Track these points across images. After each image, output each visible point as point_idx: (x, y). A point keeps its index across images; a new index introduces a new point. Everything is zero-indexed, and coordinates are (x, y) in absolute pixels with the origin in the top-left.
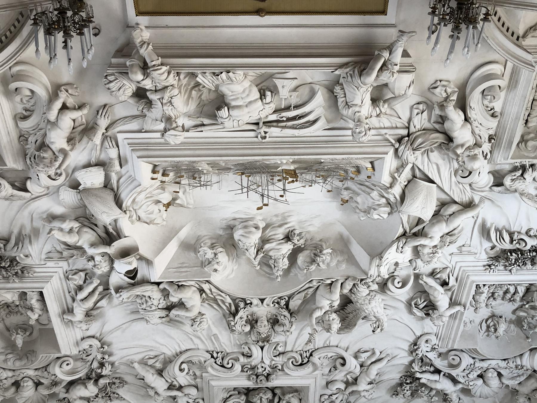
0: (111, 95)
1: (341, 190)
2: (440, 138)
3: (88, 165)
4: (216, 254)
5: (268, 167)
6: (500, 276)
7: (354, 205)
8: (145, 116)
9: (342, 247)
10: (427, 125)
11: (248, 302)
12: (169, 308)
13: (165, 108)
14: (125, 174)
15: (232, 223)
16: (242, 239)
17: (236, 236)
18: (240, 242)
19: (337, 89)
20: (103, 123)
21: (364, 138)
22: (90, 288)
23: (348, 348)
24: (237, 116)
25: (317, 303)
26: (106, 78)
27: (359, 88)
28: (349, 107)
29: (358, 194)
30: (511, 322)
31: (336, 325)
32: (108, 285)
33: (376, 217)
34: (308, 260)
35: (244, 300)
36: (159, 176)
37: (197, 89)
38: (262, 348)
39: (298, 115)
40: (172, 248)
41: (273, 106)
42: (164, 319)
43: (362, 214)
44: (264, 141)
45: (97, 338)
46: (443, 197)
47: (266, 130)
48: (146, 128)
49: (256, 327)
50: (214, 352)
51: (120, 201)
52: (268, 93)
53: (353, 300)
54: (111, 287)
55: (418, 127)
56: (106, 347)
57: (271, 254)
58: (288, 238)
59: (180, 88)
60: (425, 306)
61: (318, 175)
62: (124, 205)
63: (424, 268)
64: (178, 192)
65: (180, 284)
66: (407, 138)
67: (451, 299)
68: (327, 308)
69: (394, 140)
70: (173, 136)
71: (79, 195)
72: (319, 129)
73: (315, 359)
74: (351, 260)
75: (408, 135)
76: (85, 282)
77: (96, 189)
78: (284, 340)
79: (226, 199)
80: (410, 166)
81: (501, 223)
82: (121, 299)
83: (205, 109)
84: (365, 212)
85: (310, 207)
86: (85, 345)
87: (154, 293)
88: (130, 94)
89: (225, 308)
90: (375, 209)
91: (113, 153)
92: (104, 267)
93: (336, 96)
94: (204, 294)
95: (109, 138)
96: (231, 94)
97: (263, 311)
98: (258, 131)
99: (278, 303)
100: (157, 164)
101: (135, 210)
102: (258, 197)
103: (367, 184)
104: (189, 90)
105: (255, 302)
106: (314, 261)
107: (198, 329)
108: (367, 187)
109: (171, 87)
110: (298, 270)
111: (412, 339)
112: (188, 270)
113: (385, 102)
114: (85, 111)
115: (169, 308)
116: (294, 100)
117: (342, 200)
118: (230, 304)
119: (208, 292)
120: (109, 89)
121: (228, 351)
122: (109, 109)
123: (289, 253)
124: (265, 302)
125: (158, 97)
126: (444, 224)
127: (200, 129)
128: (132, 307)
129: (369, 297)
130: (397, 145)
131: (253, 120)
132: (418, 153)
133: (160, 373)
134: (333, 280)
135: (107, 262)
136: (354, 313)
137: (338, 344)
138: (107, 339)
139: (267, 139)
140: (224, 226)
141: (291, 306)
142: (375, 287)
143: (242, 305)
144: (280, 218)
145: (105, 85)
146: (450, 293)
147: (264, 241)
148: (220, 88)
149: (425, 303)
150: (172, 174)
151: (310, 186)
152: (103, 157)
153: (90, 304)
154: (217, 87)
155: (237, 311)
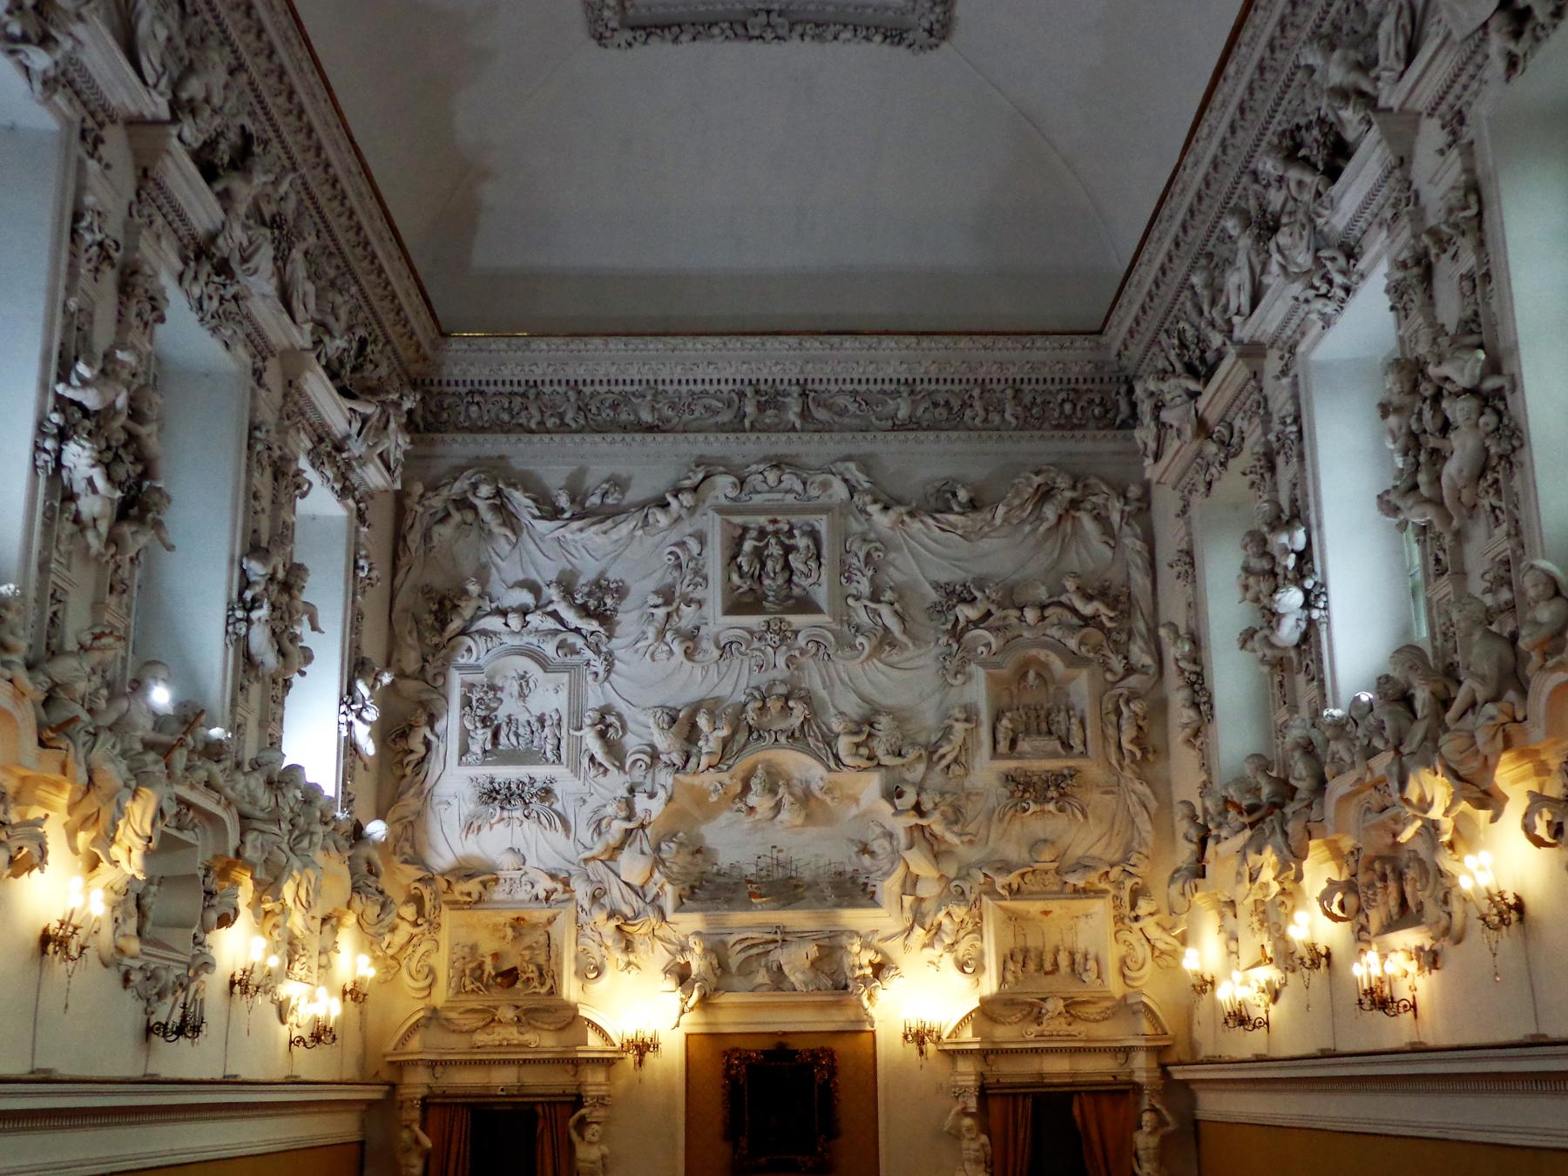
6: (540, 772)
19: (718, 972)
22: (944, 763)
30: (501, 689)
41: (772, 957)
46: (610, 863)
63: (616, 783)
81: (549, 834)
111: (613, 676)
115: (870, 735)
142: (664, 757)
143: (797, 734)
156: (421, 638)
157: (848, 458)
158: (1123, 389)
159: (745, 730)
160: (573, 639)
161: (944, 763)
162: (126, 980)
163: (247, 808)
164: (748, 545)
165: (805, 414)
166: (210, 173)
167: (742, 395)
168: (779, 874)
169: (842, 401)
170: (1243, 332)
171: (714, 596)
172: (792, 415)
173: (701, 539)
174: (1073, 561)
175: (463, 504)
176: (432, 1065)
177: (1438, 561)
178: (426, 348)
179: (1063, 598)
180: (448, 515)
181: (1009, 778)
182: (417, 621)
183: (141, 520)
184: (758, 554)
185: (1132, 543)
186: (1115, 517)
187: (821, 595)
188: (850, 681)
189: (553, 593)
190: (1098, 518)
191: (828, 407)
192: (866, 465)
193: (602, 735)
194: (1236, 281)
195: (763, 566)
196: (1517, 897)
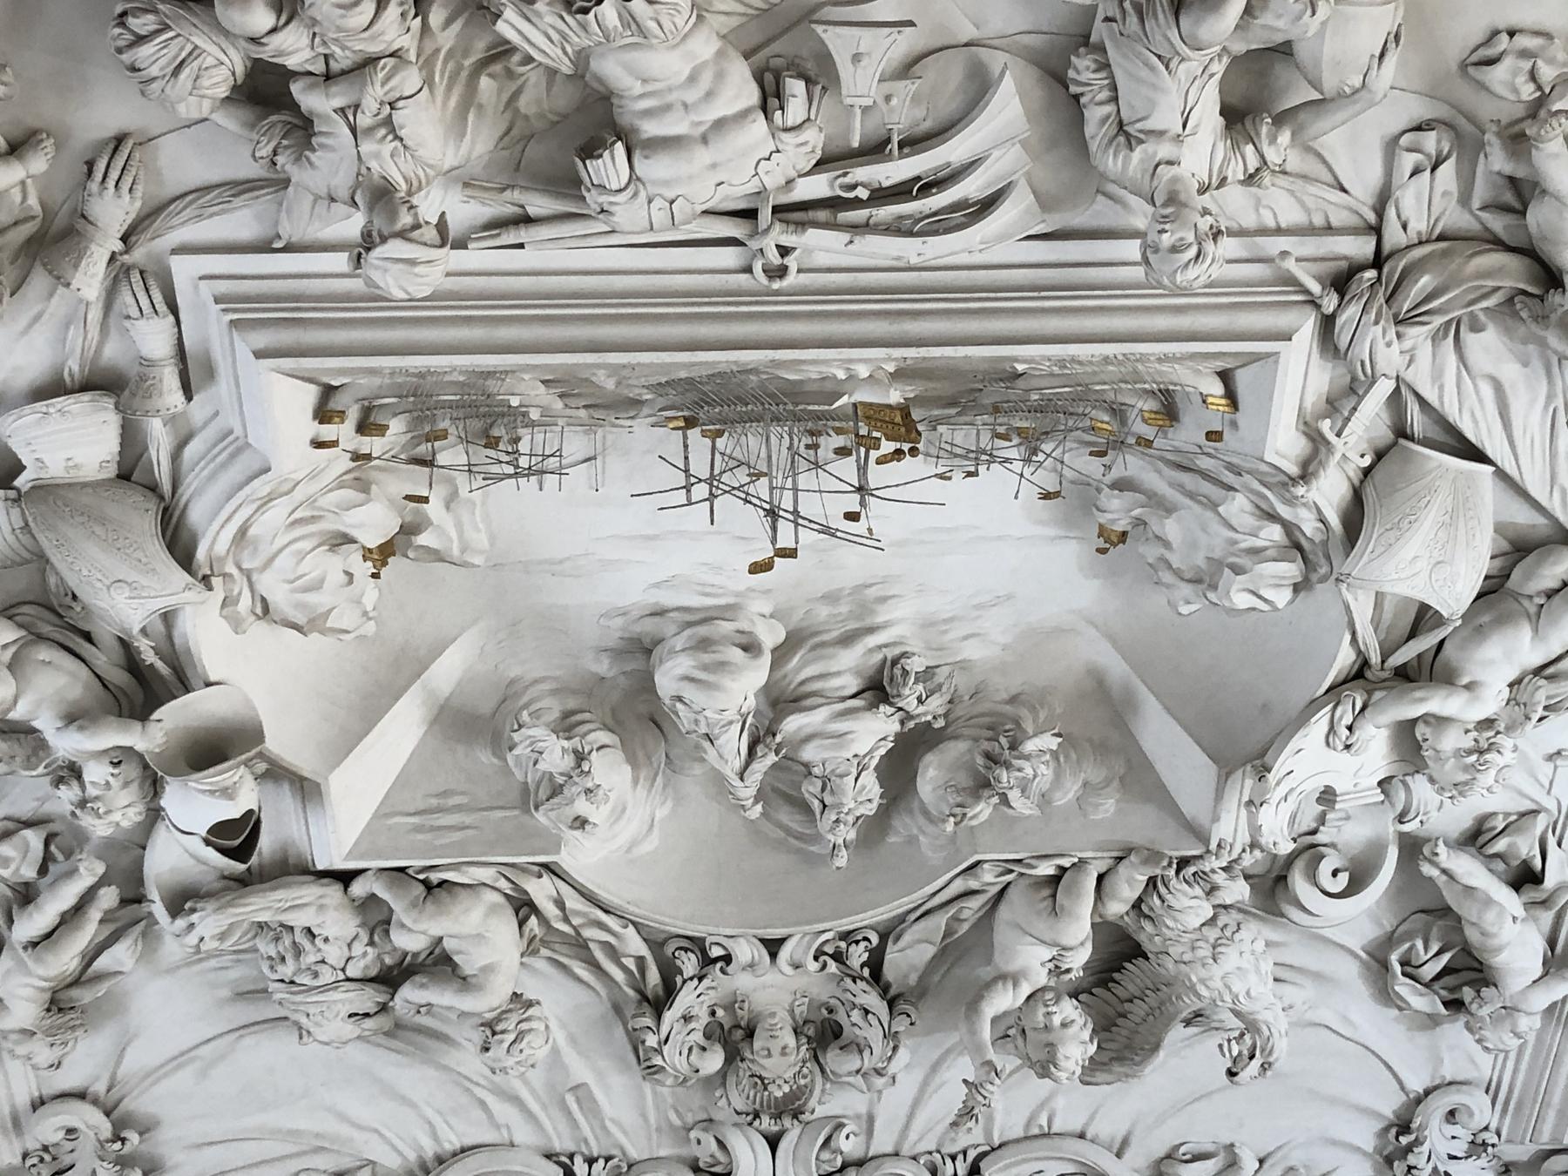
0: (143, 93)
1: (1099, 490)
2: (1509, 272)
3: (52, 389)
4: (580, 757)
5: (795, 392)
7: (1152, 552)
8: (285, 183)
9: (1102, 726)
10: (1456, 218)
11: (716, 952)
12: (390, 978)
13: (367, 147)
14: (206, 424)
15: (649, 626)
16: (689, 692)
17: (667, 680)
18: (679, 706)
19: (1082, 67)
20: (112, 211)
21: (1192, 273)
23: (1125, 1143)
24: (667, 183)
25: (997, 957)
26: (122, 24)
27: (1172, 65)
28: (1131, 142)
29: (1169, 509)
31: (1077, 1047)
32: (140, 882)
33: (1242, 600)
34: (964, 780)
35: (697, 945)
36: (344, 431)
37: (497, 68)
38: (773, 1142)
39: (918, 178)
40: (402, 730)
41: (815, 139)
42: (369, 1024)
43: (1186, 590)
44: (776, 285)
45: (95, 1102)
46: (1523, 516)
47: (788, 240)
48: (290, 230)
49: (748, 1054)
50: (578, 1160)
51: (184, 535)
52: (795, 87)
53: (1147, 946)
54: (154, 894)
55: (1419, 225)
56: (133, 1137)
57: (809, 753)
58: (878, 689)
59: (427, 65)
60: (1446, 971)
61: (1001, 430)
62: (201, 554)
63: (1441, 814)
64: (425, 500)
65: (435, 877)
66: (1371, 274)
67: (1552, 942)
68: (1041, 978)
69: (1319, 279)
70: (401, 266)
71: (15, 512)
72: (1001, 238)
74: (1141, 780)
75: (1378, 261)
76: (43, 870)
77: (85, 485)
78: (863, 1110)
79: (622, 530)
80: (1384, 388)
82: (192, 939)
83: (534, 151)
84: (1196, 581)
85: (969, 559)
86: (48, 1128)
87: (330, 918)
88: (223, 91)
89: (619, 975)
90: (1238, 570)
91: (154, 338)
92: (123, 810)
93: (1077, 97)
94: (533, 920)
95: (136, 277)
96: (638, 88)
97: (776, 989)
98: (754, 245)
99: (838, 957)
100: (335, 383)
101: (248, 574)
102: (755, 520)
103: (1204, 463)
104: (464, 74)
105: (745, 951)
106: (987, 784)
107: (510, 1062)
108: (1205, 475)
109: (391, 61)
110: (921, 820)
111: (1389, 1104)
112: (467, 819)
113: (1280, 120)
114: (38, 163)
115: (390, 978)
116: (903, 115)
117: (1102, 532)
118: (640, 961)
119: (550, 910)
120: (134, 69)
121: (634, 1154)
122: (137, 155)
123: (883, 751)
124: (785, 953)
125: (338, 102)
126: (1525, 632)
127: (510, 237)
128: (234, 974)
129: (1212, 934)
130: (1330, 303)
131: (735, 194)
132: (1417, 335)
134: (1066, 862)
135: (135, 787)
136: (1152, 999)
137: (1087, 1124)
138: (138, 1104)
139: (792, 279)
140: (612, 641)
141: (889, 972)
142: (1237, 891)
143: (689, 964)
144: (844, 609)
145: (120, 51)
146: (1547, 917)
147: (781, 701)
148: (594, 65)
149: (1446, 957)
150: (396, 426)
151: (970, 474)
152: (113, 353)
153: (66, 959)
154: (582, 59)
155: (670, 990)
159: (895, 983)
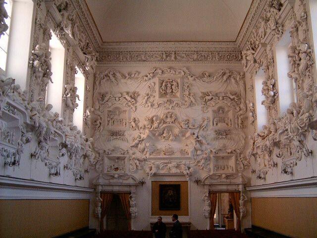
22: (203, 128)
73: (157, 106)
133: (192, 102)
138: (202, 112)
156: (99, 102)
157: (185, 67)
158: (240, 53)
160: (130, 104)
161: (203, 128)
162: (46, 164)
163: (67, 134)
164: (164, 84)
165: (175, 58)
166: (60, 11)
167: (163, 54)
168: (170, 150)
169: (183, 55)
170: (263, 41)
171: (157, 94)
172: (173, 58)
173: (155, 83)
174: (229, 88)
175: (107, 76)
176: (102, 186)
177: (299, 86)
178: (100, 44)
179: (227, 95)
180: (104, 78)
181: (216, 131)
182: (98, 99)
183: (47, 77)
184: (166, 85)
185: (241, 83)
186: (238, 79)
187: (178, 94)
188: (183, 113)
189: (125, 94)
190: (234, 79)
191: (181, 56)
192: (188, 69)
193: (135, 122)
194: (261, 30)
195: (167, 88)
196: (312, 151)
